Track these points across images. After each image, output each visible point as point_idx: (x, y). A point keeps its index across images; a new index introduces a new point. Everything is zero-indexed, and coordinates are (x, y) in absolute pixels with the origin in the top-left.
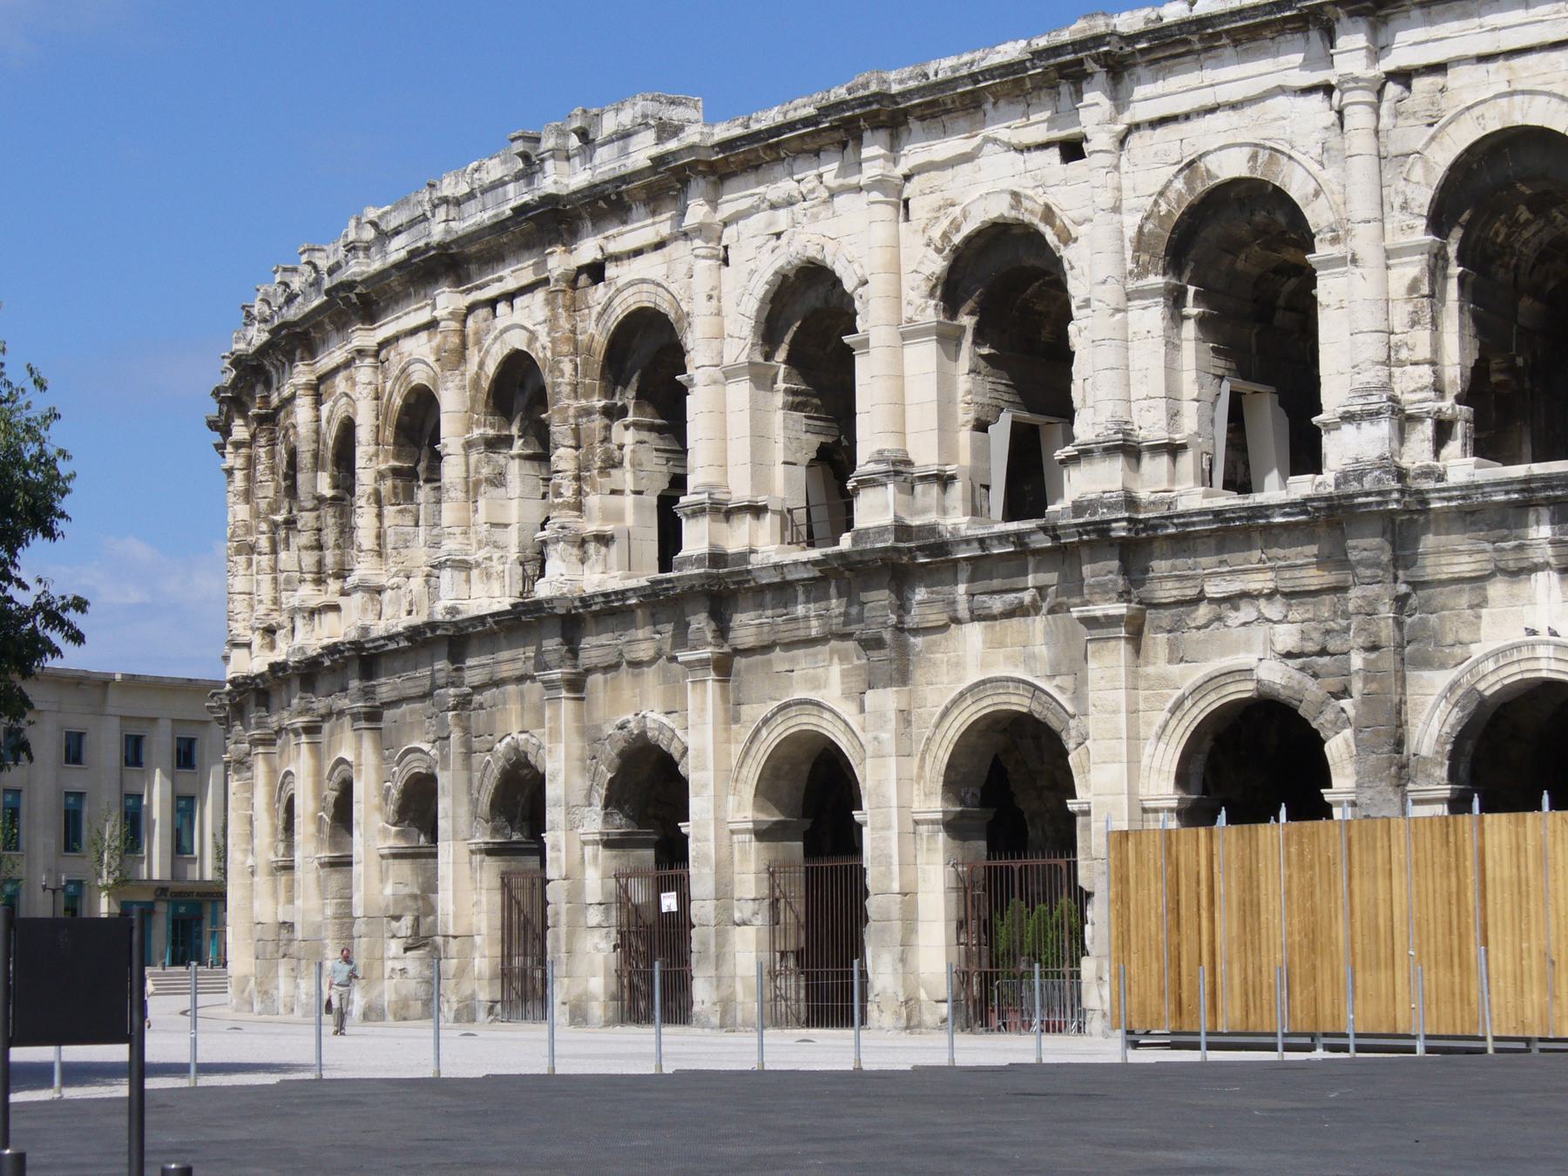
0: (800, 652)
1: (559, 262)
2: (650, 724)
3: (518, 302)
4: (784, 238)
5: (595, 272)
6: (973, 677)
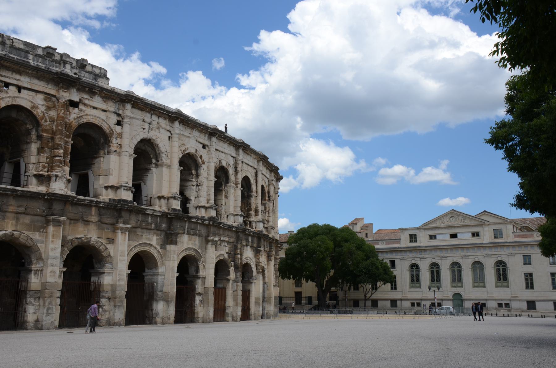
0: (145, 231)
1: (66, 95)
2: (92, 239)
3: (24, 92)
4: (146, 131)
5: (74, 104)
6: (186, 246)
